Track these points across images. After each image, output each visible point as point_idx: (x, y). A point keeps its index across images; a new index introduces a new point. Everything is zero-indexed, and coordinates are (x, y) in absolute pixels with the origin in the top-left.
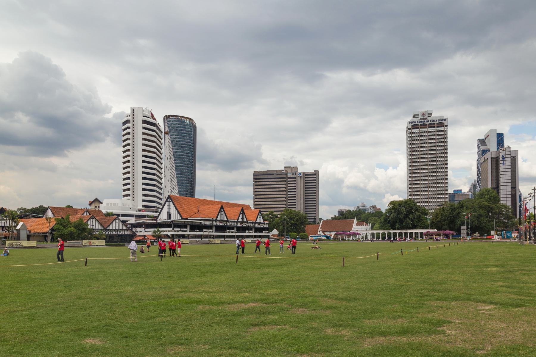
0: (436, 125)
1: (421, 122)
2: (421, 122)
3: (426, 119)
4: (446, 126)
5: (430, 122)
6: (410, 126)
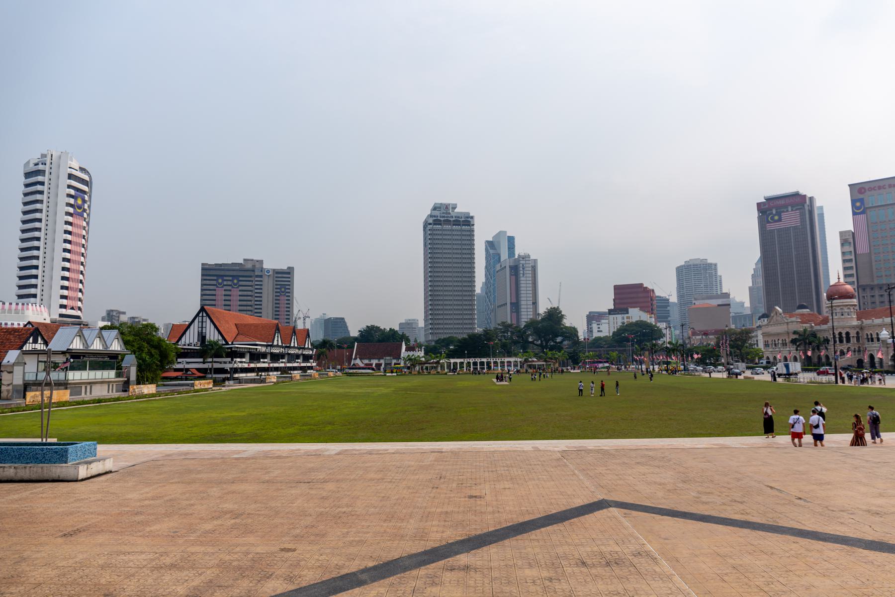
6: (431, 221)
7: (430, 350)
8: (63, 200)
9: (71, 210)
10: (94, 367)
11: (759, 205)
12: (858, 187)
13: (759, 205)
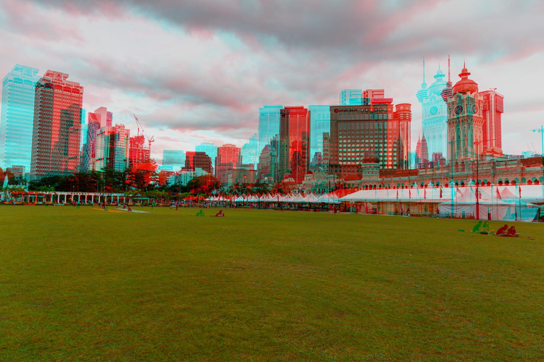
0: (72, 91)
1: (55, 82)
2: (55, 82)
3: (61, 81)
4: (82, 94)
5: (65, 86)
7: (33, 186)
11: (281, 110)
12: (335, 108)
13: (281, 110)
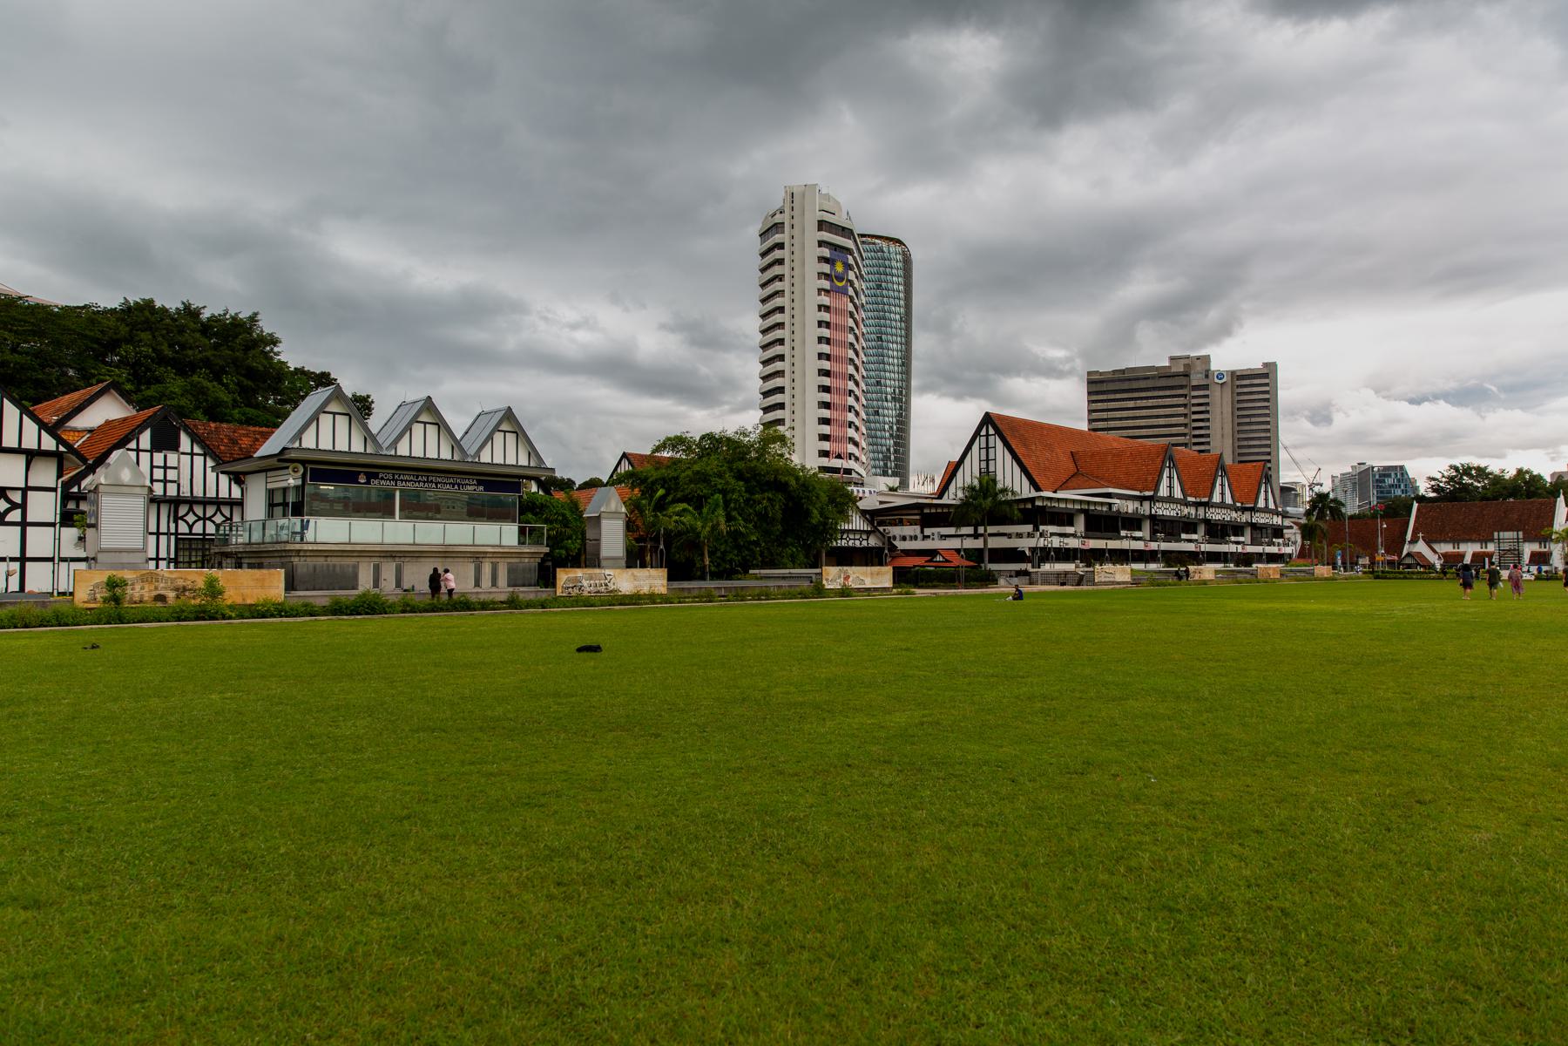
8: (813, 267)
9: (826, 284)
10: (417, 509)
